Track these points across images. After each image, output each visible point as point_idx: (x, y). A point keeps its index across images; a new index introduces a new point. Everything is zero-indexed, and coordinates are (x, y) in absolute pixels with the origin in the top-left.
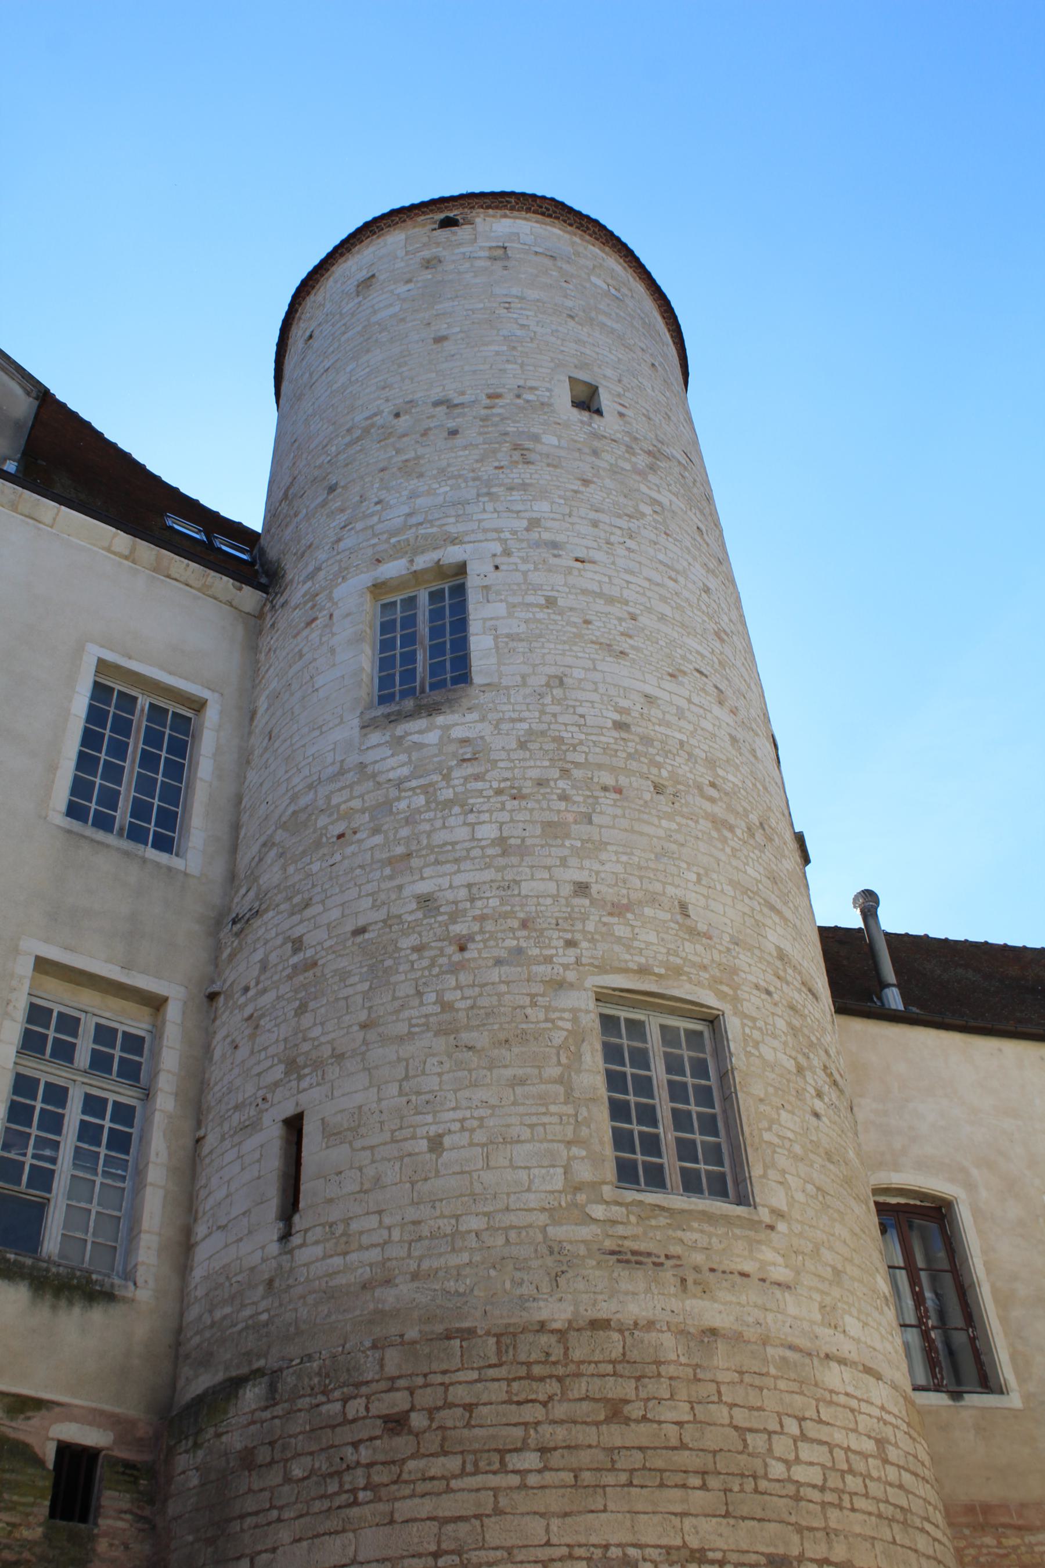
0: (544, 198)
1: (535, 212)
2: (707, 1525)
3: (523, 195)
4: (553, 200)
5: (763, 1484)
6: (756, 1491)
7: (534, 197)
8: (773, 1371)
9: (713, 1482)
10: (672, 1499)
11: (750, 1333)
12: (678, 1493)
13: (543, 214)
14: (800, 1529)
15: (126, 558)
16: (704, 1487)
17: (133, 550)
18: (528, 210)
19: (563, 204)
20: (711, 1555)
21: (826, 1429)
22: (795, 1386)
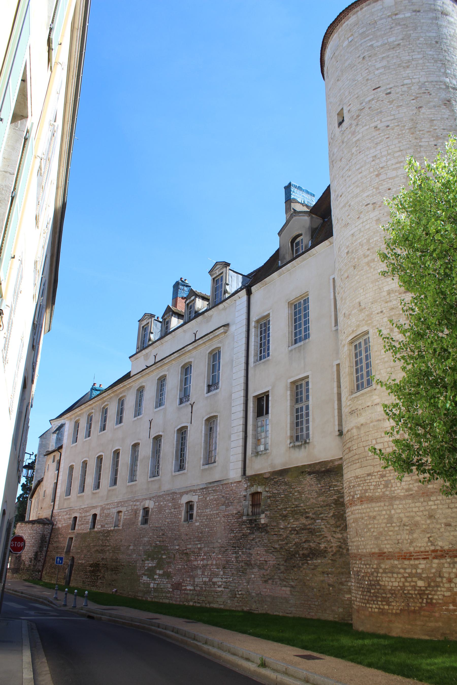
0: (327, 30)
1: (330, 36)
2: (358, 470)
3: (324, 37)
4: (329, 27)
5: (368, 458)
6: (366, 460)
7: (326, 33)
8: (371, 430)
9: (360, 461)
10: (354, 466)
11: (368, 422)
12: (355, 465)
13: (331, 34)
14: (374, 466)
15: (331, 244)
16: (358, 462)
17: (330, 242)
18: (329, 38)
19: (331, 24)
20: (359, 476)
21: (382, 439)
22: (375, 431)
